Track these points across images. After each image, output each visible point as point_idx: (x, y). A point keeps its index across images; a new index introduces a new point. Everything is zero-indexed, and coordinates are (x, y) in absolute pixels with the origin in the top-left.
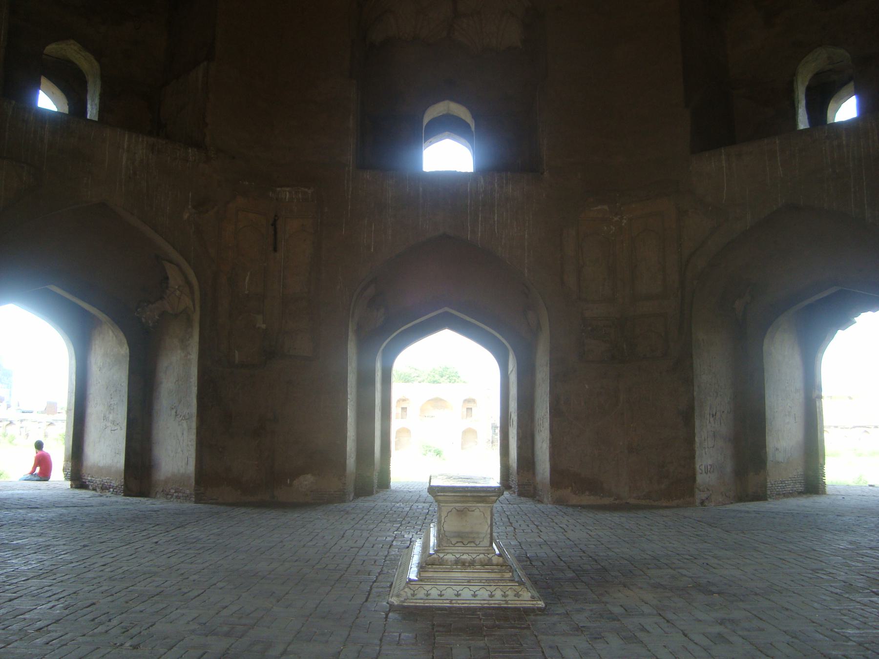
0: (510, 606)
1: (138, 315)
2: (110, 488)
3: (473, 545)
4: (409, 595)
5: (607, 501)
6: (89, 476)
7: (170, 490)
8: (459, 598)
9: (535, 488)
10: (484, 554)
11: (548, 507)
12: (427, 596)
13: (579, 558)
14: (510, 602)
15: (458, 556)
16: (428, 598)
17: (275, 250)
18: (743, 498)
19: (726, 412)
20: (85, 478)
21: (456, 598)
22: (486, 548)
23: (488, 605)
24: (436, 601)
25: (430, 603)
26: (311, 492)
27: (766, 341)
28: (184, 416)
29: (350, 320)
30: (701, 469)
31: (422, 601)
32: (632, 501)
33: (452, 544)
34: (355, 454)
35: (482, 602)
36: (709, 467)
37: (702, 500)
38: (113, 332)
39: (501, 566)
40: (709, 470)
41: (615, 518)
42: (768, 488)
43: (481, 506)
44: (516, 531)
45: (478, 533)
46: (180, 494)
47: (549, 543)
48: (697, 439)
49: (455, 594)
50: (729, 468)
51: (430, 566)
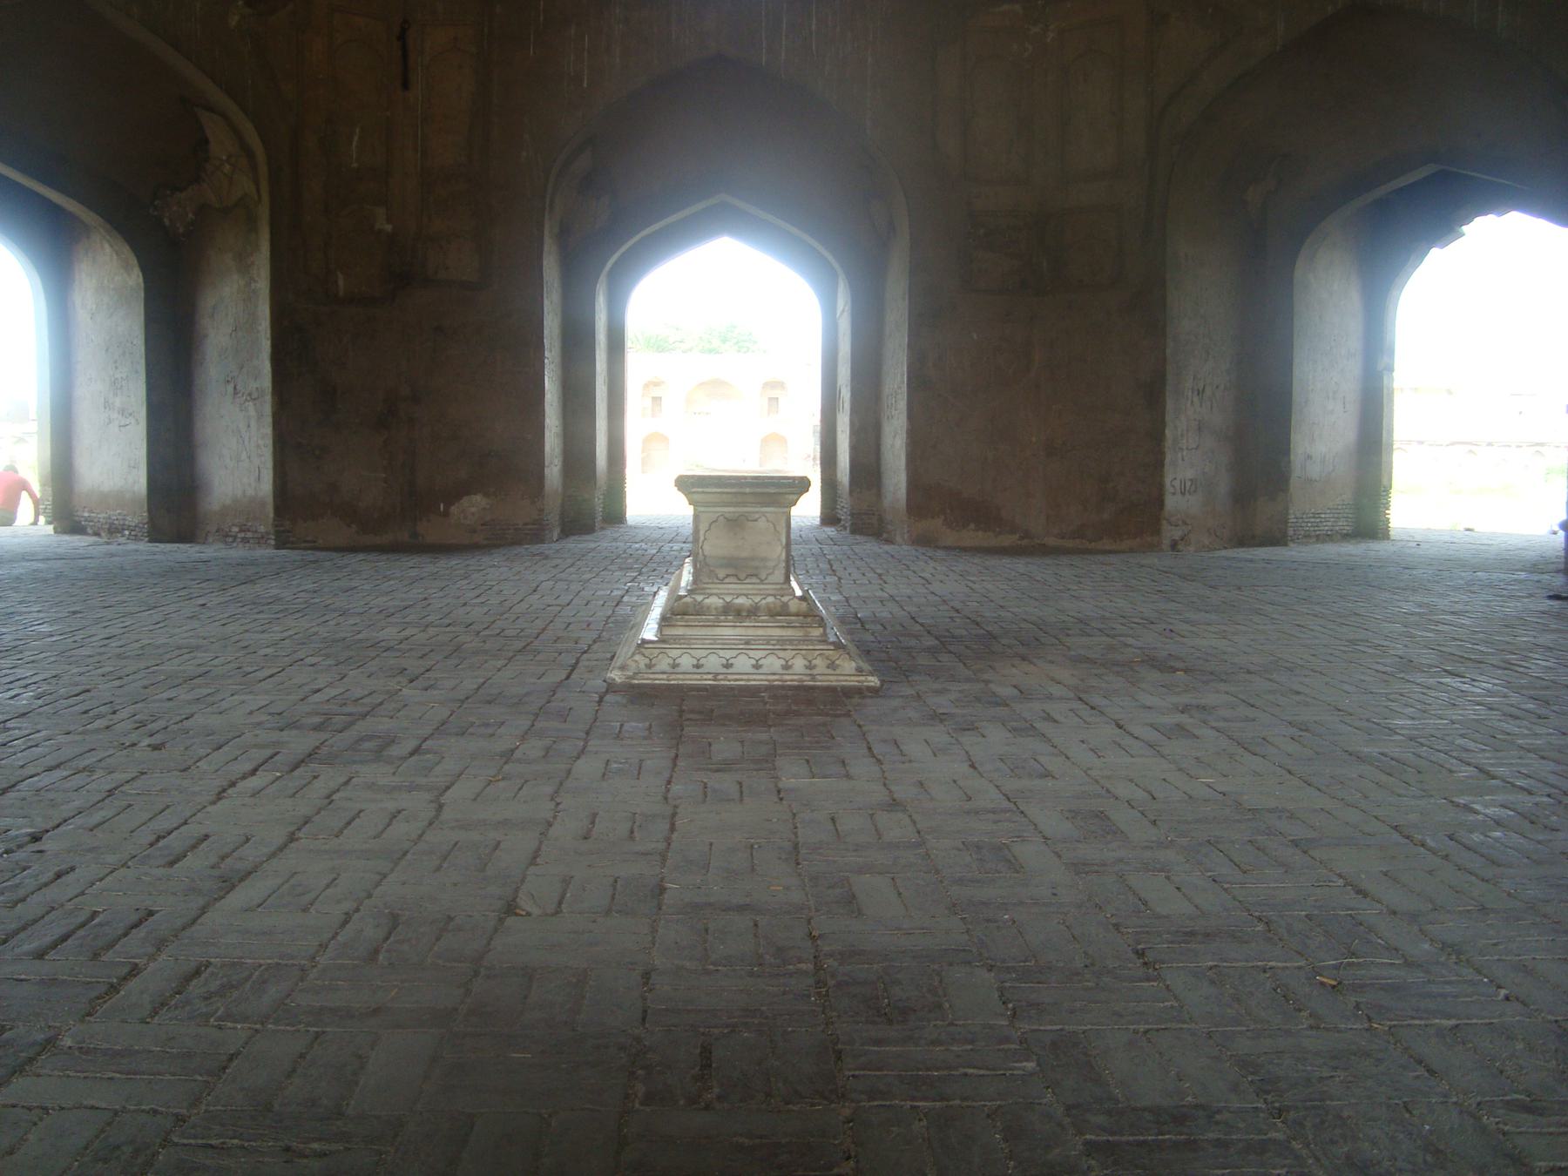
1: (156, 213)
2: (123, 529)
3: (754, 580)
4: (642, 666)
5: (1007, 540)
6: (86, 509)
7: (230, 527)
8: (730, 671)
9: (881, 520)
10: (774, 596)
11: (904, 550)
13: (949, 620)
14: (819, 677)
15: (728, 599)
16: (675, 671)
17: (406, 85)
18: (1244, 540)
19: (1222, 387)
20: (79, 513)
21: (725, 670)
22: (778, 587)
23: (780, 683)
24: (688, 676)
26: (482, 525)
27: (1300, 263)
28: (250, 394)
29: (547, 217)
30: (1173, 486)
31: (665, 676)
32: (1051, 541)
33: (717, 578)
34: (561, 459)
36: (1188, 484)
37: (1174, 540)
38: (111, 246)
39: (805, 616)
40: (1187, 488)
41: (1021, 565)
42: (1290, 524)
43: (771, 513)
44: (842, 581)
45: (764, 559)
46: (249, 535)
47: (897, 599)
48: (1168, 432)
49: (723, 665)
50: (1223, 485)
51: (679, 617)
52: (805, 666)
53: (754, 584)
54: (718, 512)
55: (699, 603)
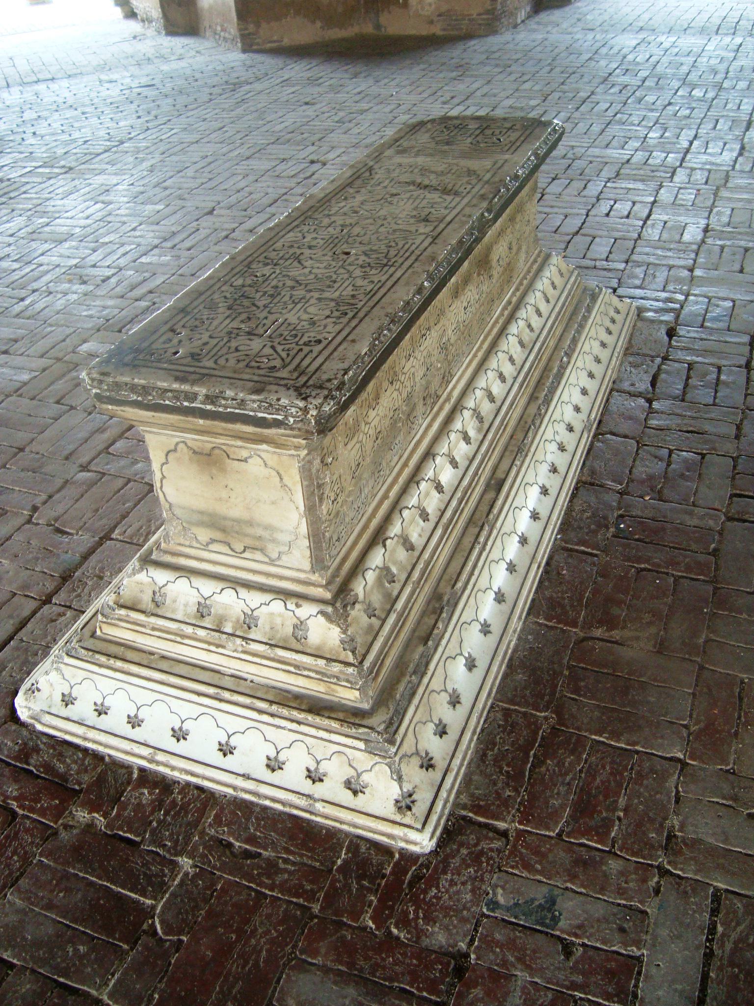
0: (318, 819)
3: (258, 556)
10: (285, 595)
12: (100, 714)
14: (319, 806)
21: (171, 744)
25: (101, 744)
26: (439, 15)
31: (80, 730)
35: (240, 782)
46: (227, 35)
51: (123, 612)
52: (308, 770)
53: (262, 562)
54: (172, 436)
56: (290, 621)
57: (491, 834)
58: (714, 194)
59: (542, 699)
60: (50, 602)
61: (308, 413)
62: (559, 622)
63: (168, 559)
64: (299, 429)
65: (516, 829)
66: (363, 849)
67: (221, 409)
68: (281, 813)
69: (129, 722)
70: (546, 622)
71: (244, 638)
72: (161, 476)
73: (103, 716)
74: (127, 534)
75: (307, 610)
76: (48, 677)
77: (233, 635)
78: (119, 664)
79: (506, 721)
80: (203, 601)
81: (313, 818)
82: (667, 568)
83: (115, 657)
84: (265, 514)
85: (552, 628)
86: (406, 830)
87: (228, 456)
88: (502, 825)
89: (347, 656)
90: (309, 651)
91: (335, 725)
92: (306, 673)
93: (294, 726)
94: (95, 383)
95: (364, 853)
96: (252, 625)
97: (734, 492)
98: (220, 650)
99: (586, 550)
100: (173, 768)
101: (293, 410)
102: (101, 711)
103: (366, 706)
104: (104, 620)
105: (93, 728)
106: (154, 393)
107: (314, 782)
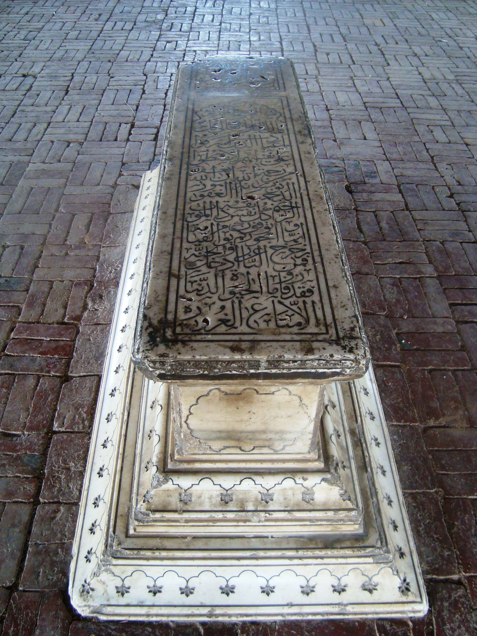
0: (350, 617)
4: (112, 591)
12: (155, 594)
14: (349, 609)
21: (223, 599)
35: (286, 610)
45: (282, 432)
49: (221, 588)
51: (158, 515)
53: (266, 454)
55: (186, 491)
56: (299, 490)
57: (453, 586)
58: (317, 81)
59: (428, 480)
60: (39, 503)
61: (359, 363)
62: (406, 421)
63: (185, 466)
64: (350, 375)
65: (465, 577)
66: (388, 628)
67: (285, 371)
68: (322, 621)
69: (182, 593)
70: (398, 423)
71: (265, 511)
72: (188, 413)
73: (158, 594)
74: (66, 425)
75: (313, 480)
76: (99, 578)
77: (256, 511)
78: (164, 554)
79: (416, 502)
80: (225, 492)
81: (346, 617)
82: (444, 366)
83: (158, 549)
84: (279, 424)
85: (404, 426)
86: (413, 605)
87: (257, 392)
88: (455, 577)
89: (347, 504)
90: (318, 508)
91: (348, 552)
92: (319, 523)
93: (319, 561)
94: (158, 365)
95: (390, 630)
96: (268, 500)
97: (450, 302)
98: (248, 524)
99: (391, 363)
100: (230, 616)
101: (348, 363)
102: (155, 591)
103: (361, 531)
104: (142, 524)
105: (153, 606)
106: (219, 366)
107: (340, 593)
